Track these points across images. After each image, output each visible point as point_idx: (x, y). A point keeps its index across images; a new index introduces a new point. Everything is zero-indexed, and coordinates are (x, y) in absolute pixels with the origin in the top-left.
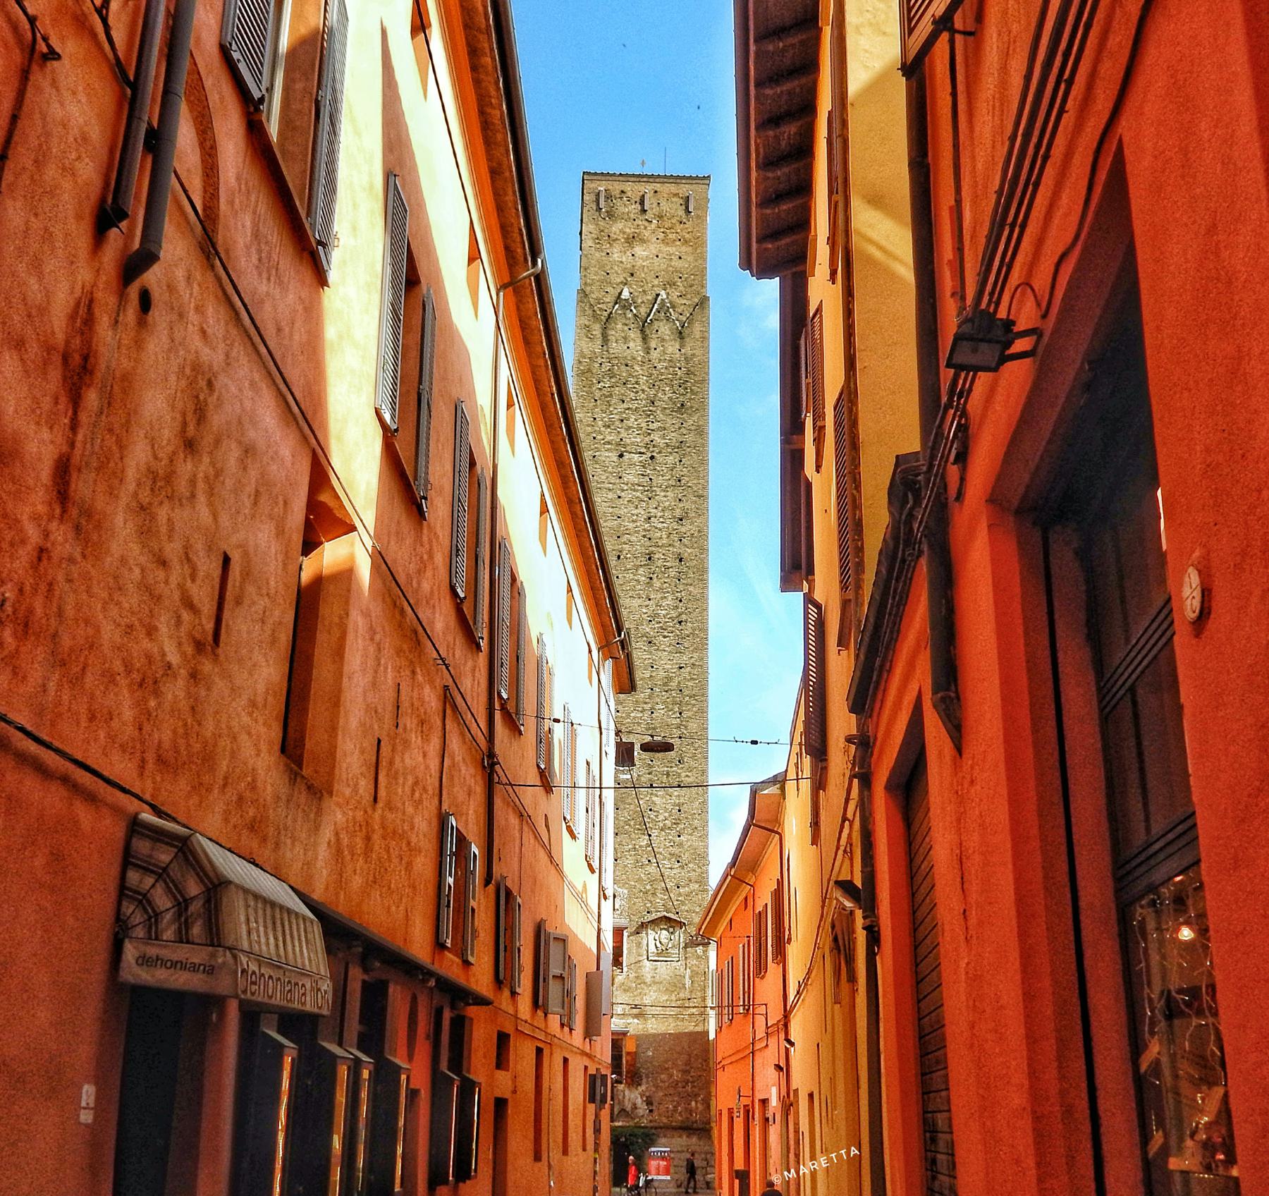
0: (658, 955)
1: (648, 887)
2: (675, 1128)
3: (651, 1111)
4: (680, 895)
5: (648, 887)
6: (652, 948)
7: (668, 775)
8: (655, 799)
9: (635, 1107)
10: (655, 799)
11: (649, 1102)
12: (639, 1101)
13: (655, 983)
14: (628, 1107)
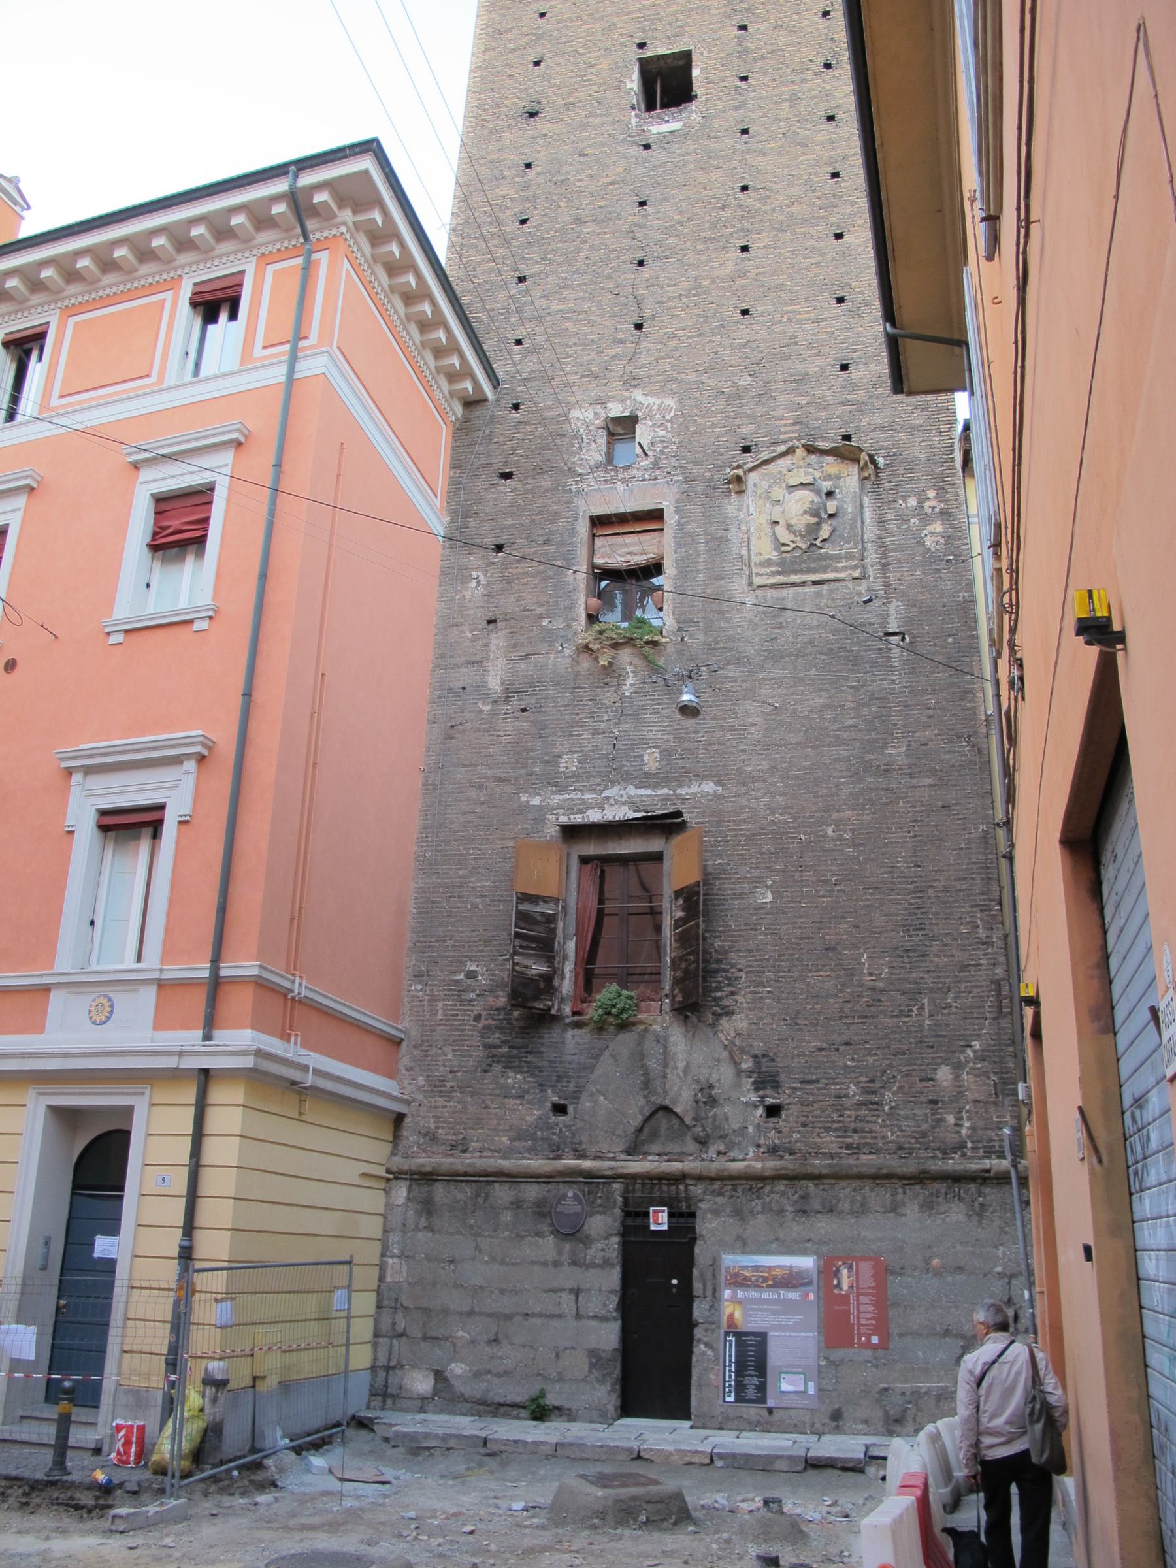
0: (785, 567)
1: (745, 380)
2: (879, 1178)
3: (773, 1111)
4: (852, 386)
5: (745, 380)
6: (763, 549)
7: (794, 99)
8: (753, 160)
9: (708, 1097)
10: (753, 160)
11: (766, 1080)
12: (724, 1075)
13: (775, 657)
14: (683, 1100)
